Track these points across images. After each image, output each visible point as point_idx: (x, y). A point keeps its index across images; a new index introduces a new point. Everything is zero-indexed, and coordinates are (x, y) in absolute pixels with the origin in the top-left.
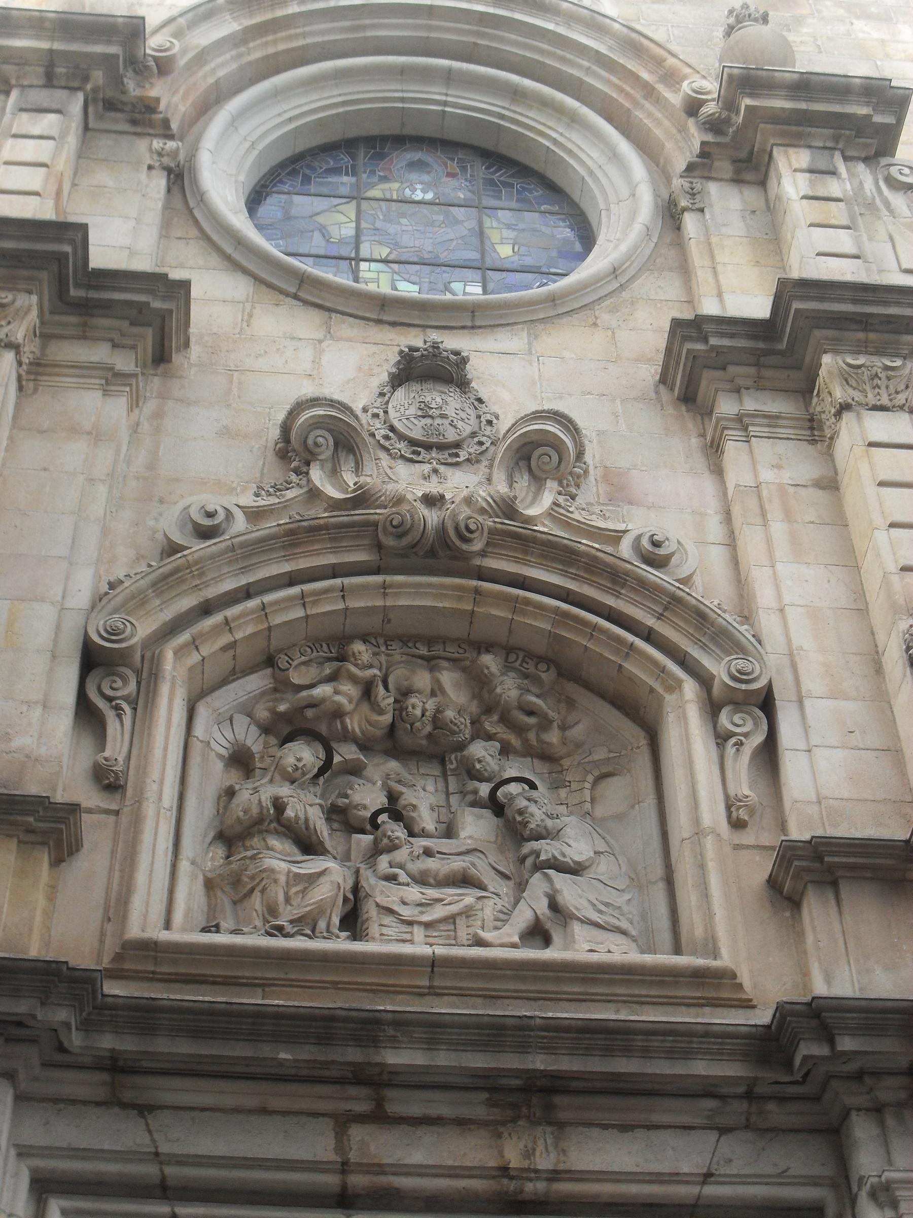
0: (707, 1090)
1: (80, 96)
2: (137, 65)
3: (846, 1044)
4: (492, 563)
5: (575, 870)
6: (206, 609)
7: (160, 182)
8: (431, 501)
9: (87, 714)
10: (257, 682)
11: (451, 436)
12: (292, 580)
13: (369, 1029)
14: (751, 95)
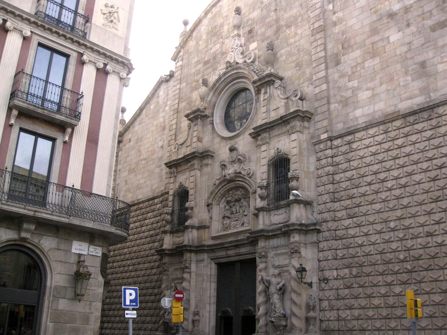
0: (247, 243)
1: (199, 120)
2: (203, 112)
3: (251, 239)
4: (237, 179)
5: (246, 216)
6: (216, 194)
7: (210, 127)
8: (229, 174)
9: (209, 211)
10: (224, 199)
11: (234, 160)
12: (223, 187)
13: (222, 244)
14: (255, 84)
